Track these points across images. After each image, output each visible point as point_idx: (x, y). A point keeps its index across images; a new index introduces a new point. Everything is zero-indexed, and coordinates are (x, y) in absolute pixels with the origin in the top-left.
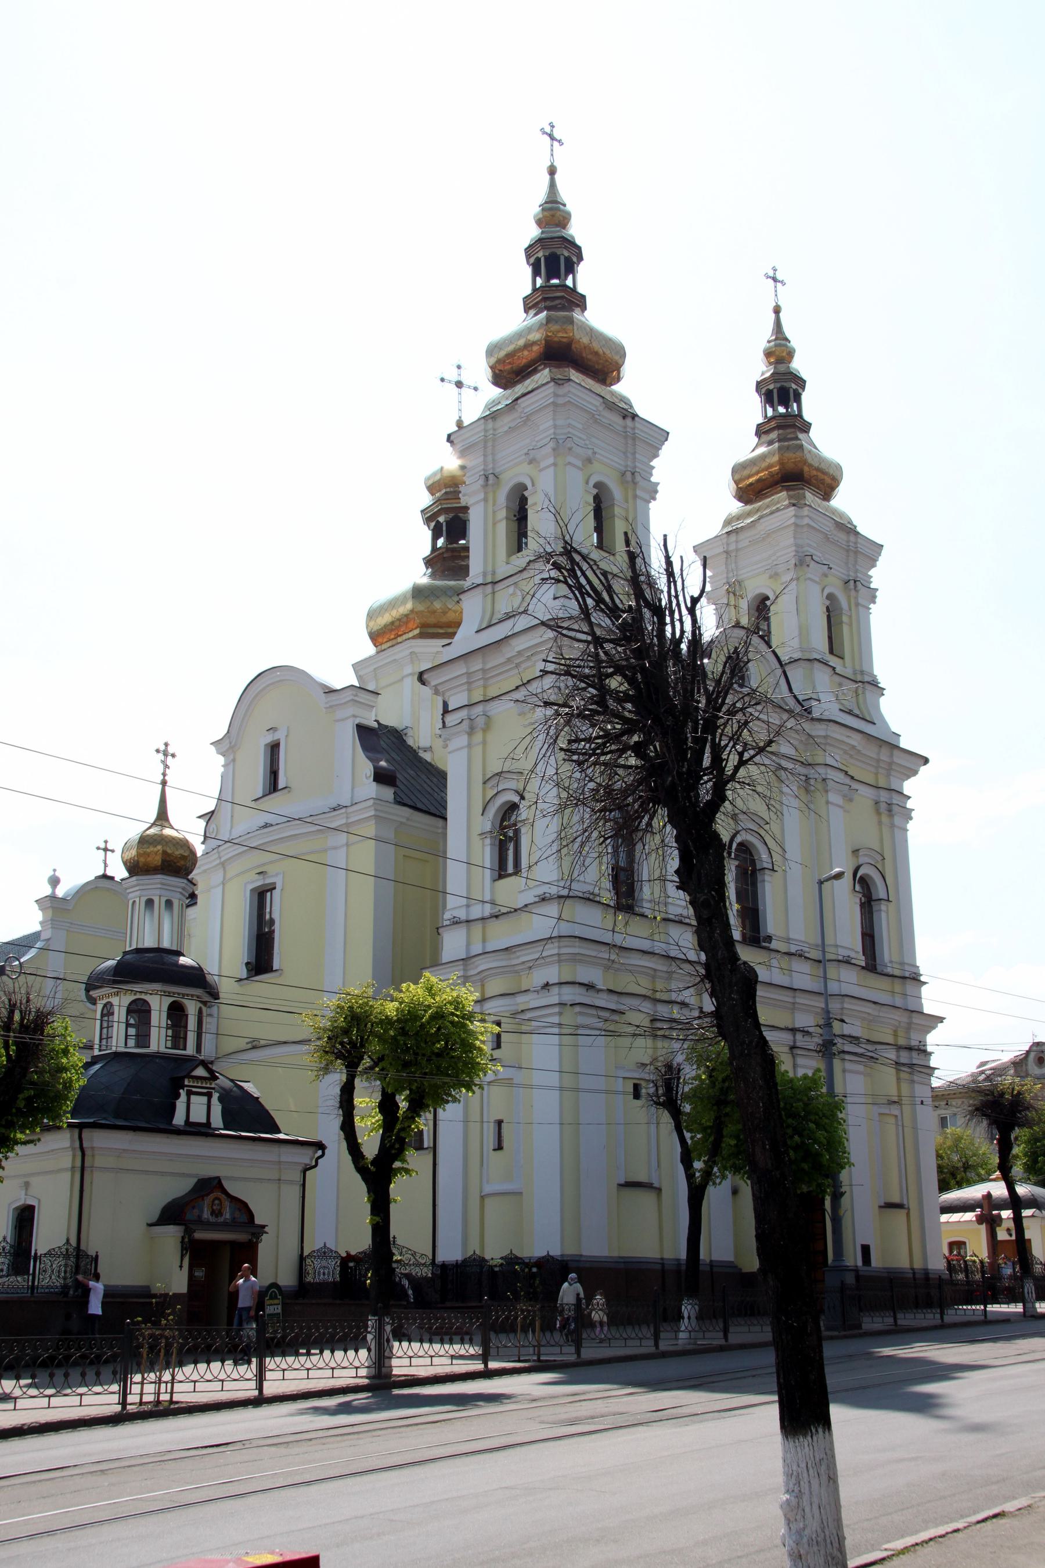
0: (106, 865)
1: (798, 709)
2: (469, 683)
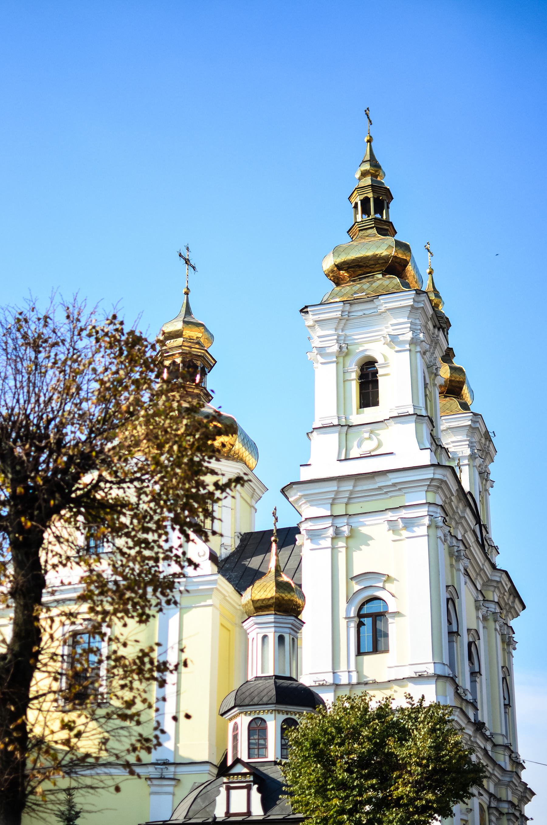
2: (334, 499)
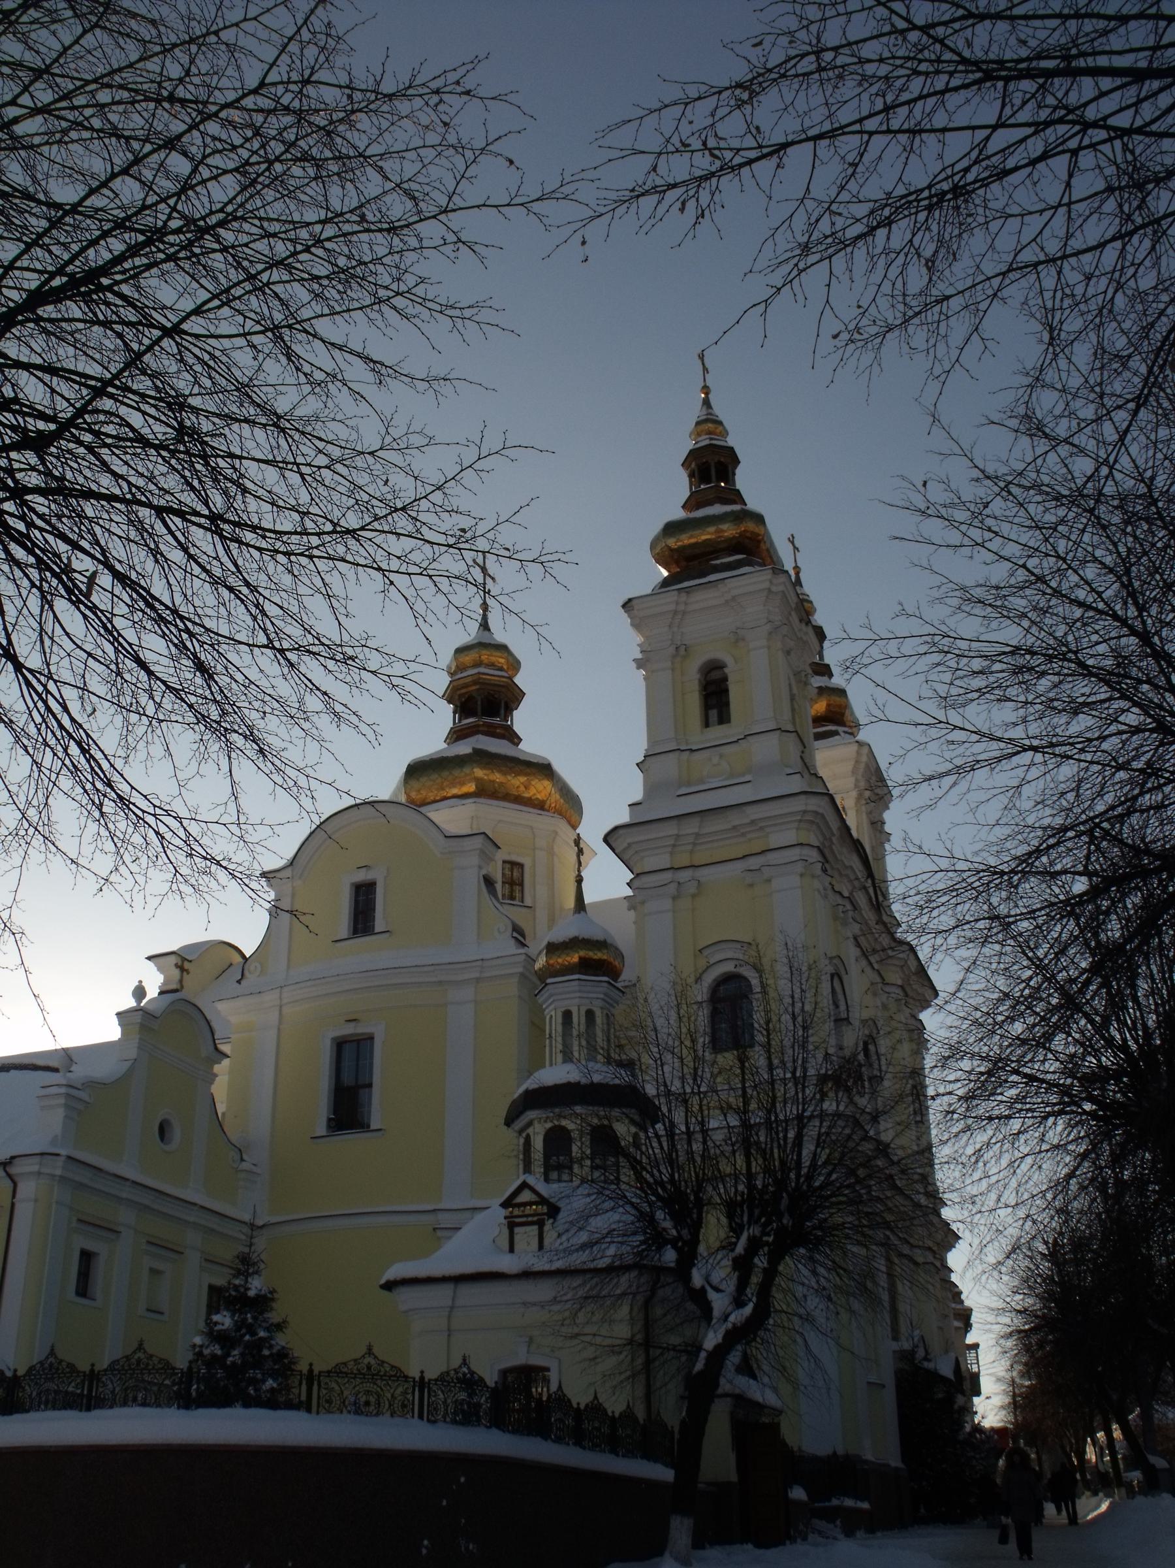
2: (674, 846)
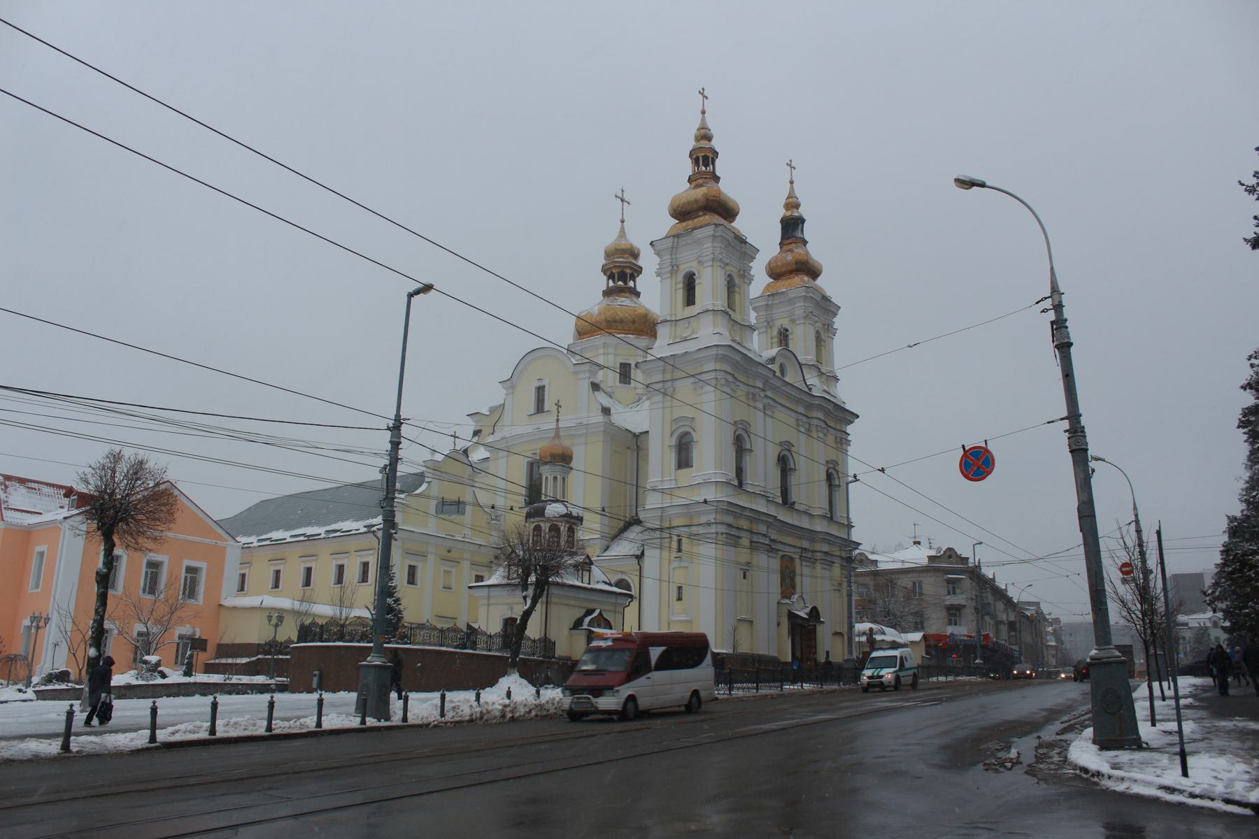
0: (455, 445)
1: (807, 390)
2: (664, 370)
